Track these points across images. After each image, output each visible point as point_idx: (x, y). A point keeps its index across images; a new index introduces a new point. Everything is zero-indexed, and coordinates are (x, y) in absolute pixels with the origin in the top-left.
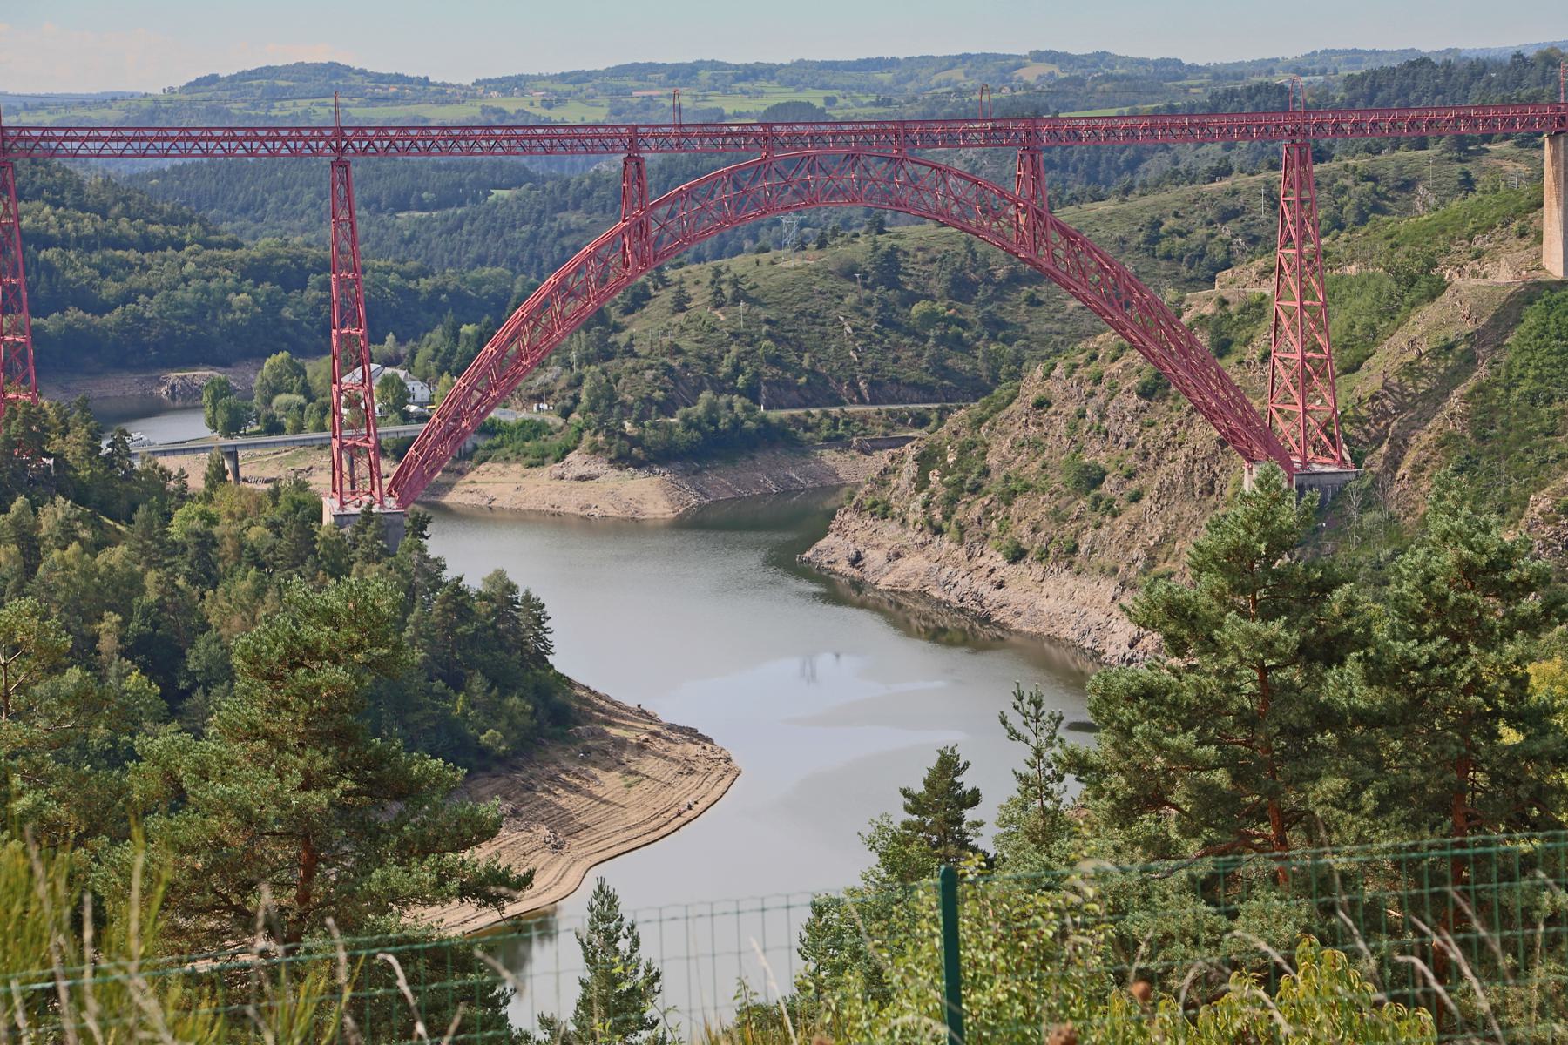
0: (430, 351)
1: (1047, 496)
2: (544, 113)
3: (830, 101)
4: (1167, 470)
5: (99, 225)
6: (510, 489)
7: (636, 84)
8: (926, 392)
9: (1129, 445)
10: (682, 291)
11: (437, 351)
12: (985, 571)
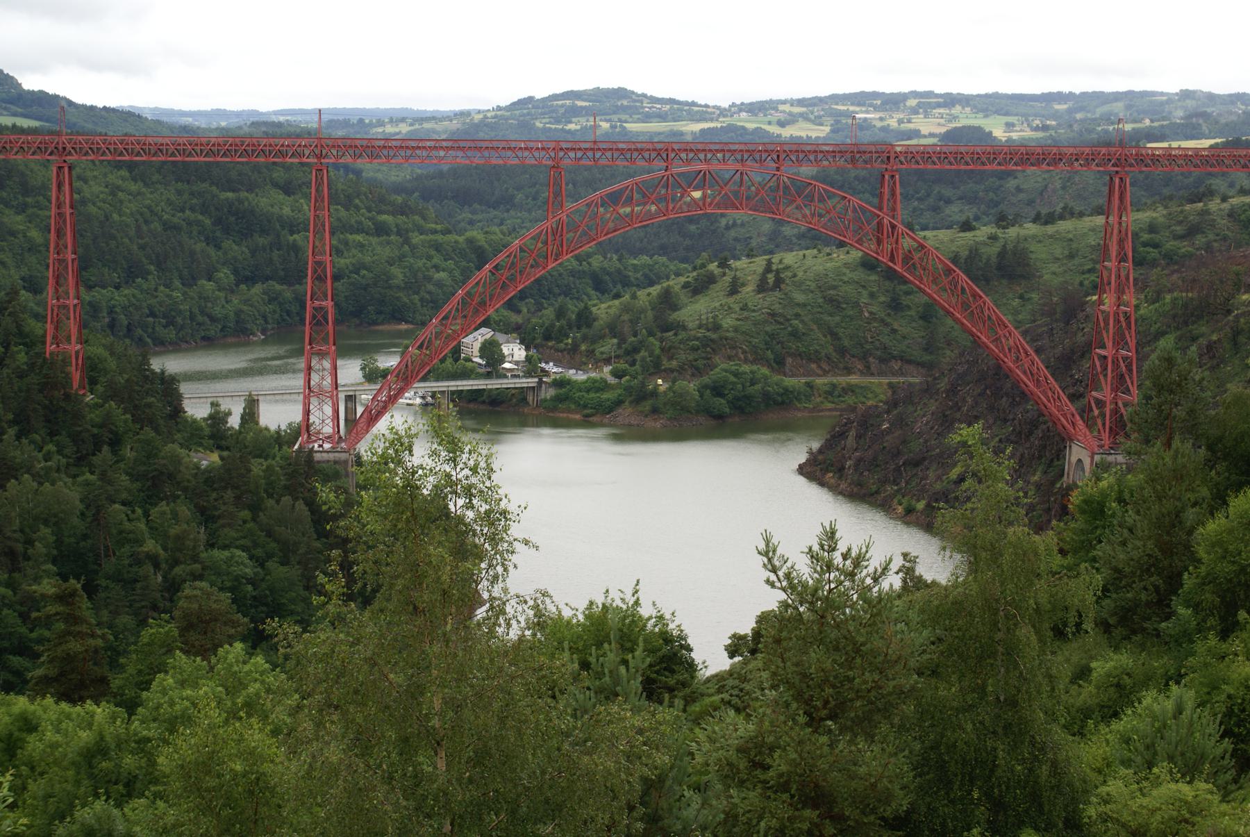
7: (857, 109)
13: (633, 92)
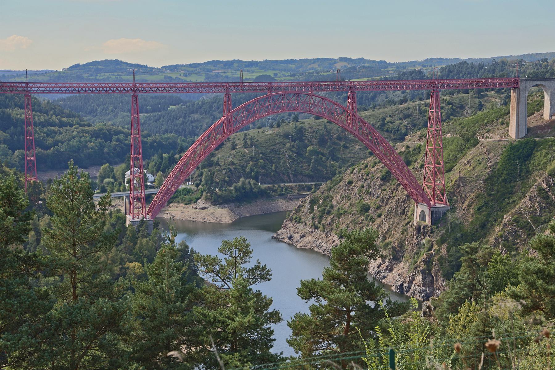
0: (154, 163)
1: (351, 215)
2: (184, 78)
3: (276, 74)
4: (390, 206)
5: (46, 117)
6: (180, 213)
7: (214, 68)
8: (311, 178)
9: (377, 197)
10: (234, 142)
11: (156, 163)
12: (331, 241)
13: (122, 62)
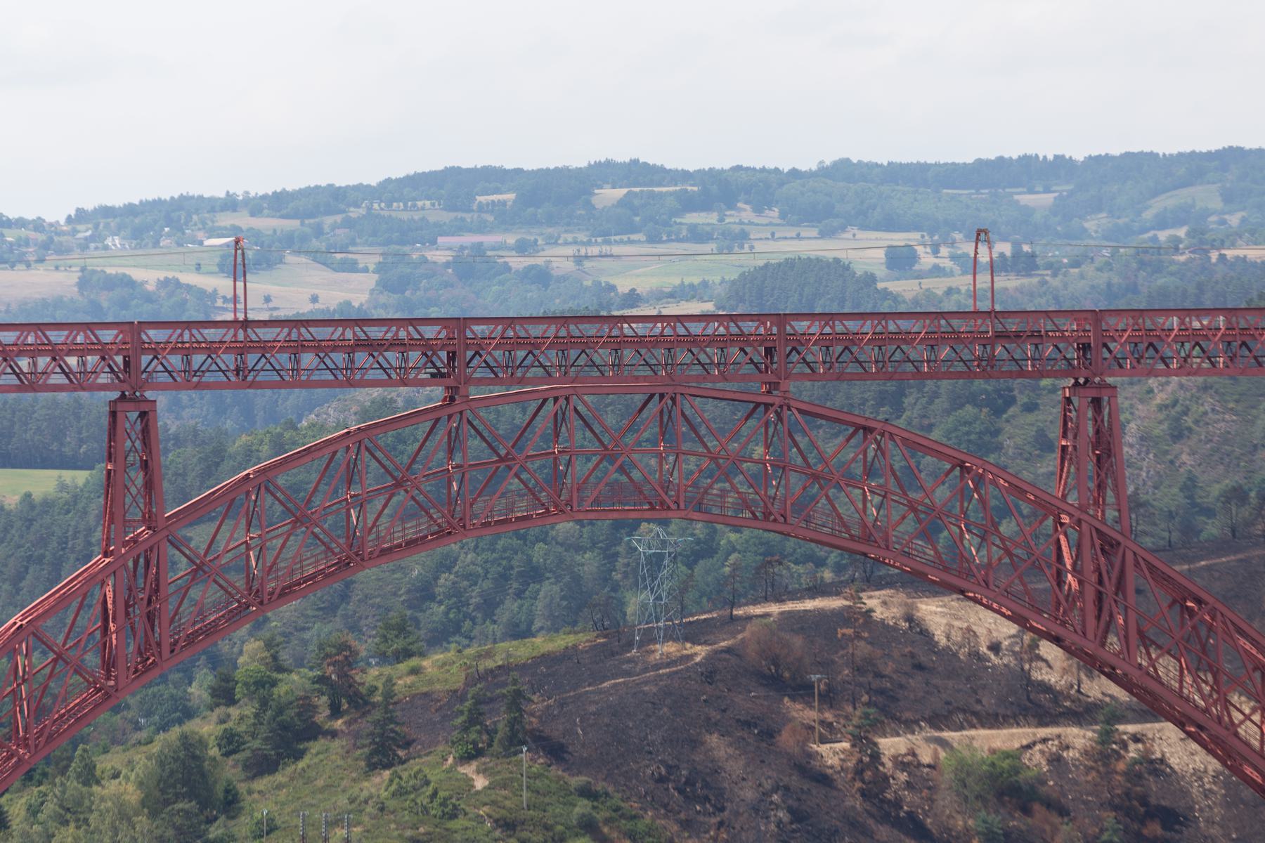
7: (446, 217)
